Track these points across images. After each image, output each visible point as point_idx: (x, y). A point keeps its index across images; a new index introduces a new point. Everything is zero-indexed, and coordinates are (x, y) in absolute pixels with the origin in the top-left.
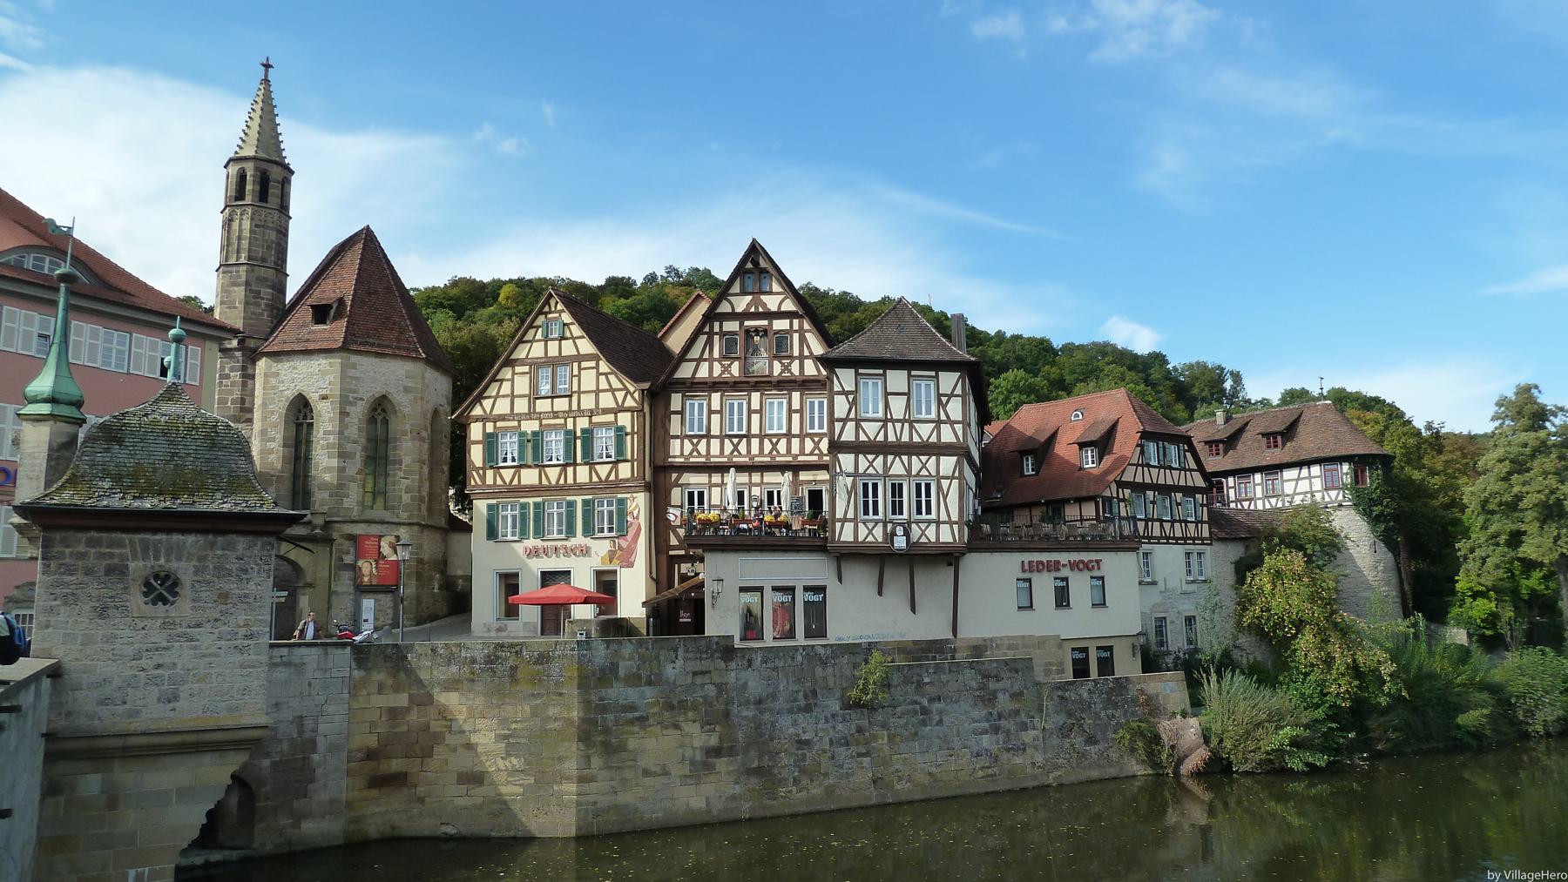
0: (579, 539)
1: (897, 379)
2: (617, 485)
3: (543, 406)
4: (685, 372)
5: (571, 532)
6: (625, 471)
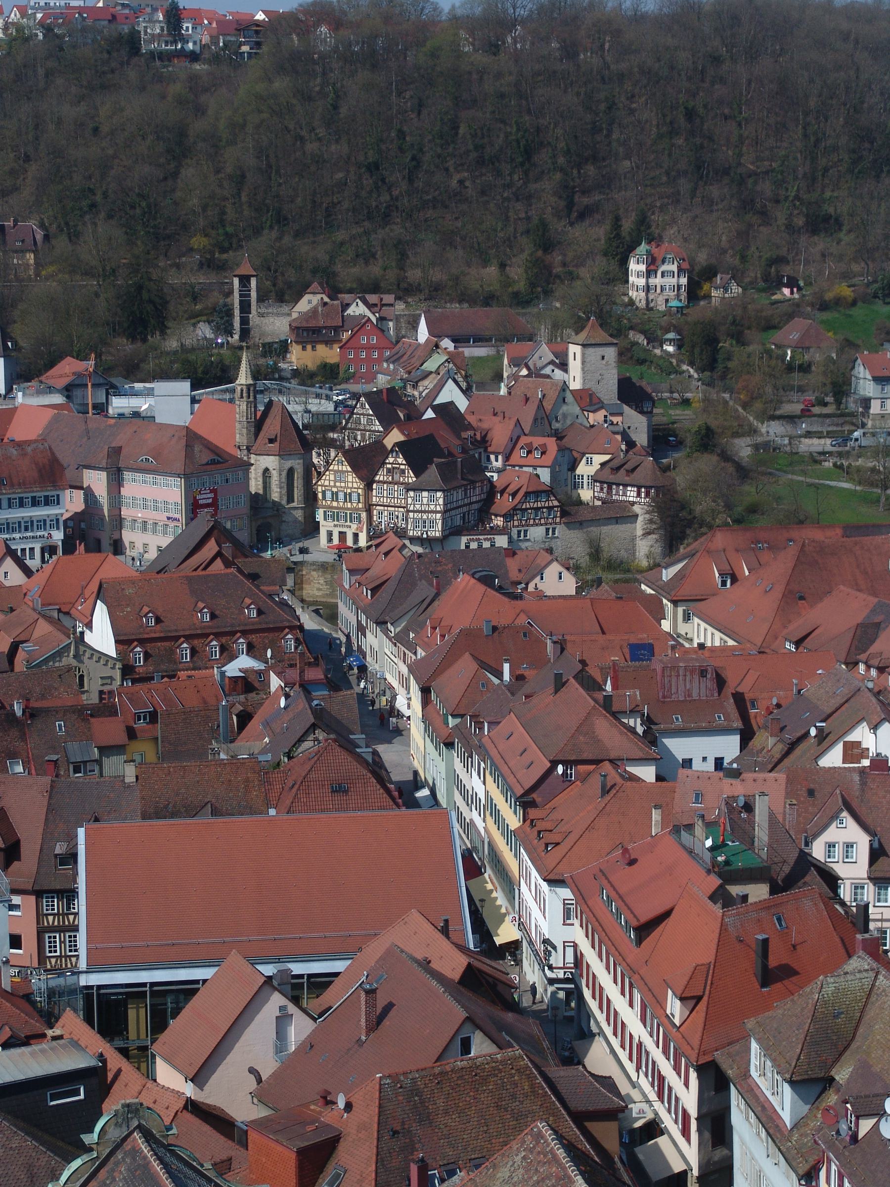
0: (348, 523)
1: (425, 494)
2: (358, 509)
3: (338, 484)
4: (377, 478)
5: (346, 521)
6: (360, 505)
